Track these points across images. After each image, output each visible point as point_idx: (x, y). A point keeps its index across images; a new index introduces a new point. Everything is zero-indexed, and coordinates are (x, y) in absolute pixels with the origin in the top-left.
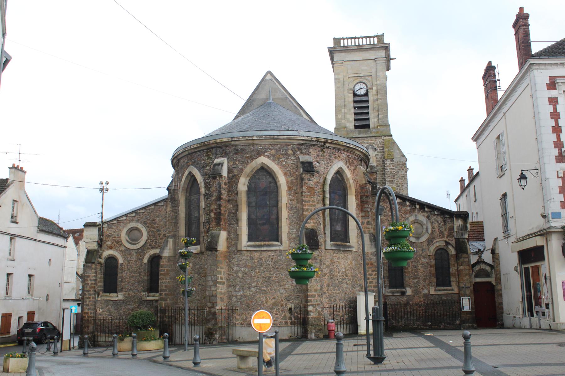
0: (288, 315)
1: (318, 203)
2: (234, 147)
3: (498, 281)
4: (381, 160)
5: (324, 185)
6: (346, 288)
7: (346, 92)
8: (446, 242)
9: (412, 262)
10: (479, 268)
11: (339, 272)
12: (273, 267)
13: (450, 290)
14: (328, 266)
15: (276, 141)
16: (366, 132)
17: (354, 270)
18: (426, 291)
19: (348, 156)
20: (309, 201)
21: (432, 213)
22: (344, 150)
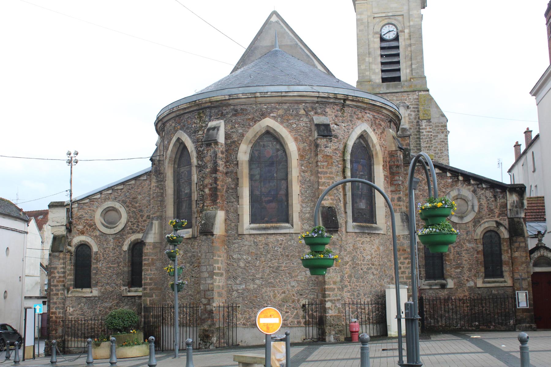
0: (301, 313)
1: (337, 175)
2: (232, 107)
4: (415, 121)
5: (344, 153)
6: (372, 279)
7: (370, 36)
8: (497, 222)
9: (454, 247)
10: (539, 255)
11: (363, 261)
12: (282, 255)
13: (501, 282)
14: (350, 253)
15: (284, 98)
16: (396, 87)
17: (382, 258)
18: (471, 284)
19: (374, 116)
20: (326, 173)
21: (480, 186)
22: (369, 109)
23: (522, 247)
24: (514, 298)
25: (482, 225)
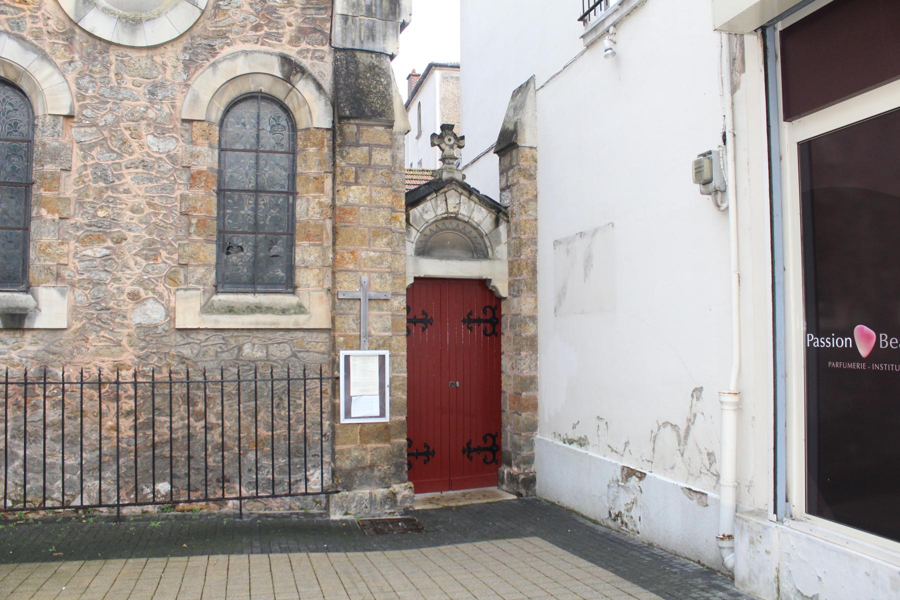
3: (525, 275)
8: (285, 60)
9: (87, 149)
10: (441, 211)
13: (284, 311)
18: (153, 313)
23: (376, 167)
24: (332, 379)
25: (223, 66)
